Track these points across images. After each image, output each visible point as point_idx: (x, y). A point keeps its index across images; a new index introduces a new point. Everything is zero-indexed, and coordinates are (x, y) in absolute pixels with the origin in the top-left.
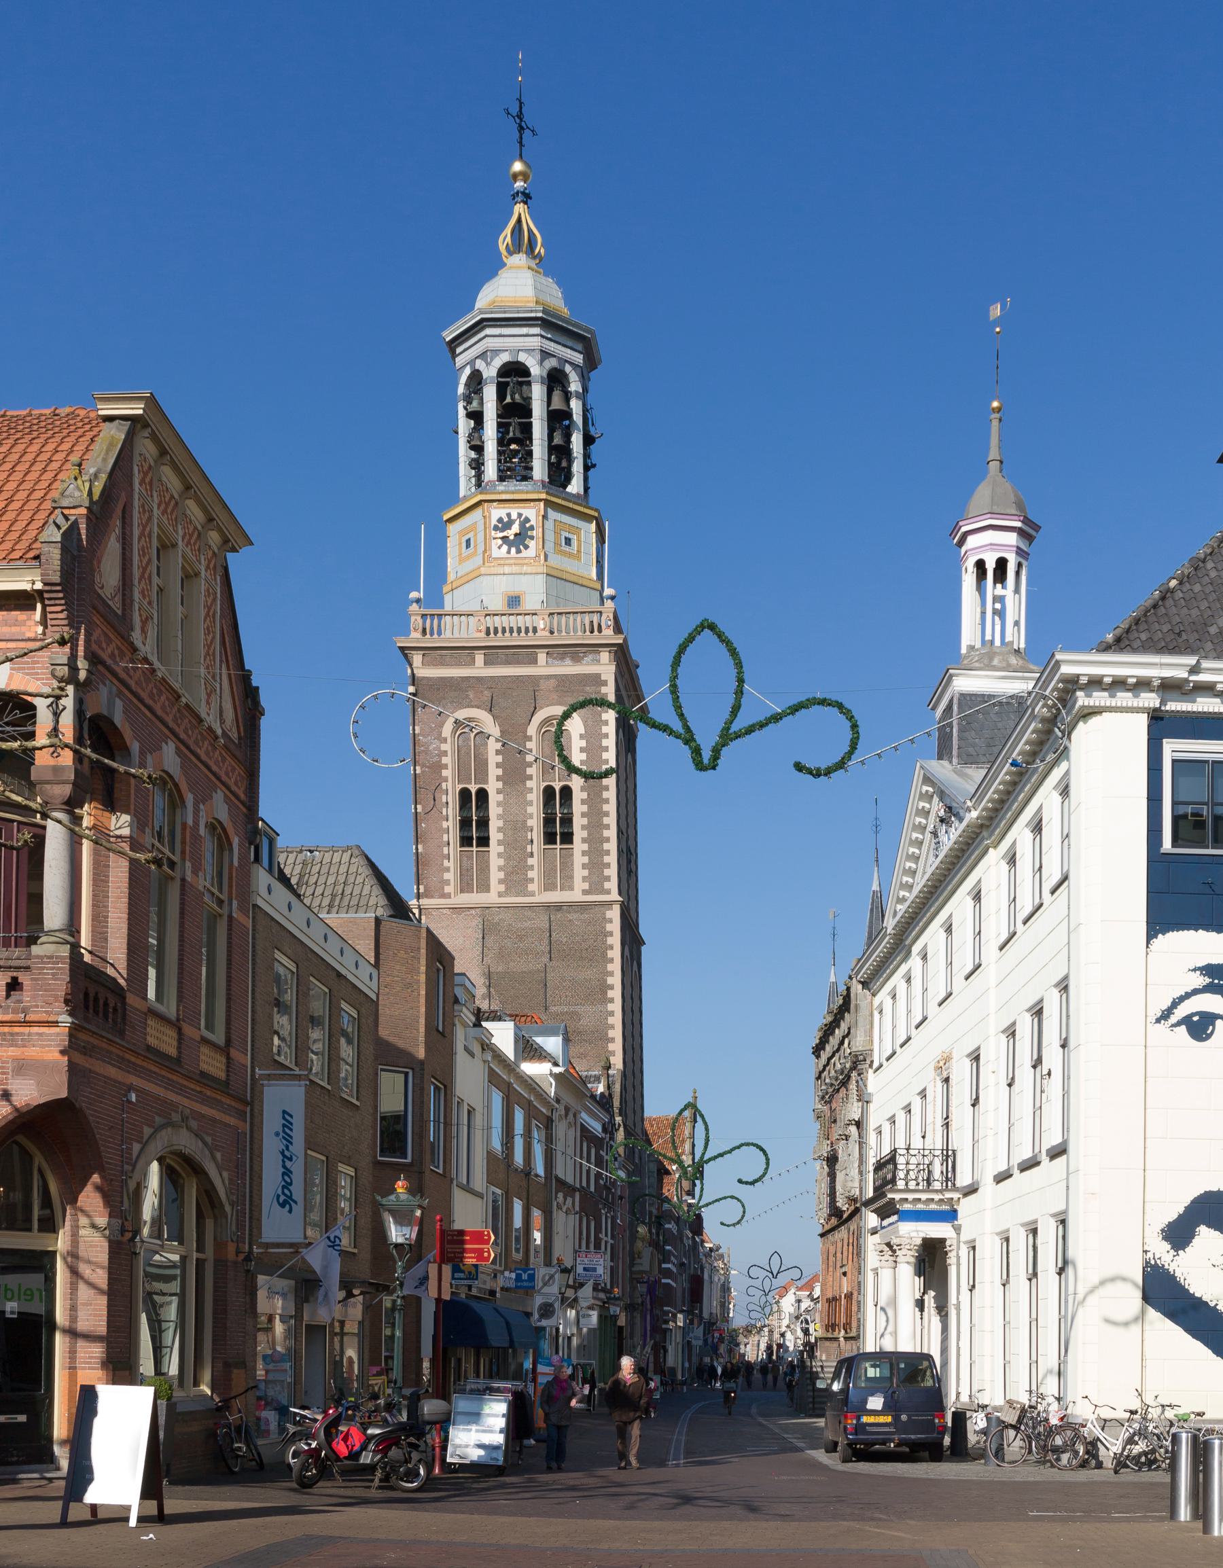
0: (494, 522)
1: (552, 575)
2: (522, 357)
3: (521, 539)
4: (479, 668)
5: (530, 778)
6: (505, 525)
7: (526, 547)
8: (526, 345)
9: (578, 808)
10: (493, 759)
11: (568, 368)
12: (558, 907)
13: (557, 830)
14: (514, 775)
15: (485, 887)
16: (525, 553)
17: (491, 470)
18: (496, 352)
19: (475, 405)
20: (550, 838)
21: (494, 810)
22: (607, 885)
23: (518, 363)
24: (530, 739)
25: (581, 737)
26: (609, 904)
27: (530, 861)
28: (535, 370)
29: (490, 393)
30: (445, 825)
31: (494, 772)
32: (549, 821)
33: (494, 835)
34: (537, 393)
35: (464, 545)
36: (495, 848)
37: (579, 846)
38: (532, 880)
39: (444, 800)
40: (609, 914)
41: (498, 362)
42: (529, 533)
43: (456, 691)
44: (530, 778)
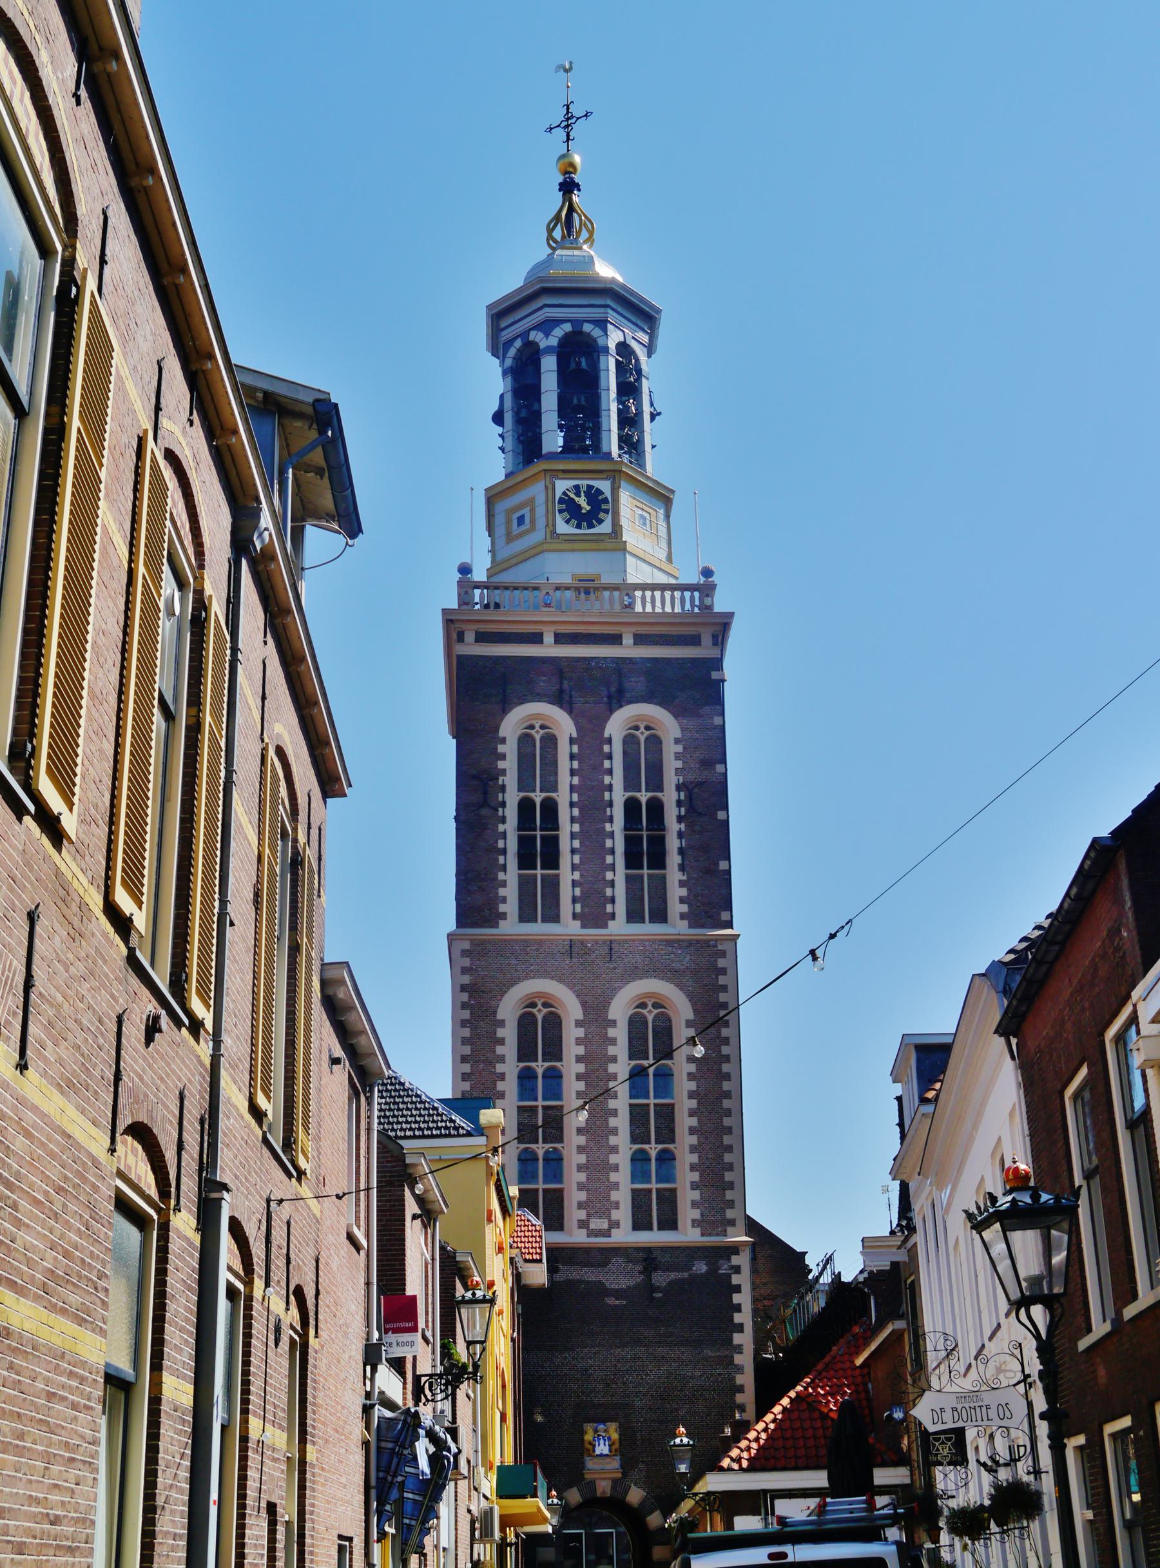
0: (558, 494)
2: (587, 328)
4: (549, 649)
7: (600, 521)
15: (553, 916)
18: (557, 322)
23: (581, 333)
29: (549, 364)
35: (515, 522)
41: (559, 332)
42: (603, 506)
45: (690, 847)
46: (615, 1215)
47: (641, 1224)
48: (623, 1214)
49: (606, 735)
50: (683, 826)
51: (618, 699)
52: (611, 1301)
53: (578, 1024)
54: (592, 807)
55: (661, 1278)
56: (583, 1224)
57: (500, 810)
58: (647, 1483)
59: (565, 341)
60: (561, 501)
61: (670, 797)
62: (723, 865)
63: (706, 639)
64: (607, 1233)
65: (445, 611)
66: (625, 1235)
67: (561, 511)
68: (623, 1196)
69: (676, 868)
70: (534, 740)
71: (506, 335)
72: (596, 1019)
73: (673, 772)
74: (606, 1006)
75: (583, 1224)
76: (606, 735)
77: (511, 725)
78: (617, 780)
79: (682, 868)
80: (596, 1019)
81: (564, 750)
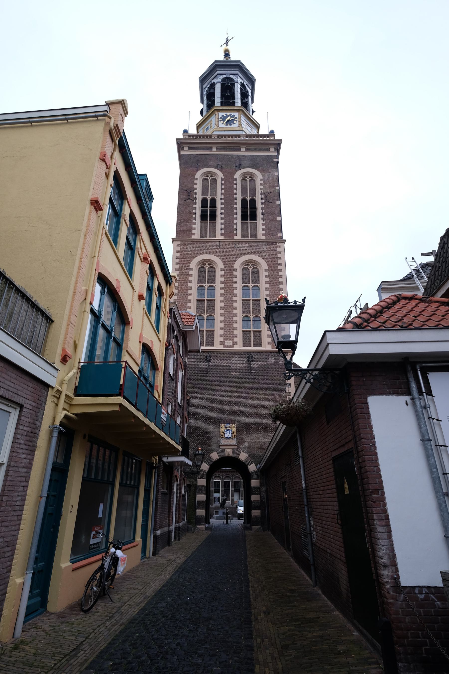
2: (231, 76)
4: (214, 152)
6: (223, 118)
31: (219, 191)
36: (219, 221)
45: (266, 212)
46: (235, 340)
47: (246, 343)
48: (239, 339)
49: (235, 178)
50: (263, 206)
51: (240, 167)
52: (233, 373)
53: (222, 270)
54: (229, 198)
55: (254, 365)
56: (222, 343)
57: (194, 200)
58: (249, 451)
59: (224, 80)
61: (258, 198)
62: (279, 218)
63: (272, 149)
64: (232, 346)
65: (177, 139)
66: (239, 347)
67: (220, 121)
68: (239, 333)
69: (261, 219)
70: (208, 180)
71: (204, 86)
72: (229, 269)
73: (260, 189)
74: (233, 263)
75: (222, 343)
76: (235, 178)
77: (199, 175)
78: (239, 191)
79: (263, 219)
80: (229, 269)
81: (219, 182)
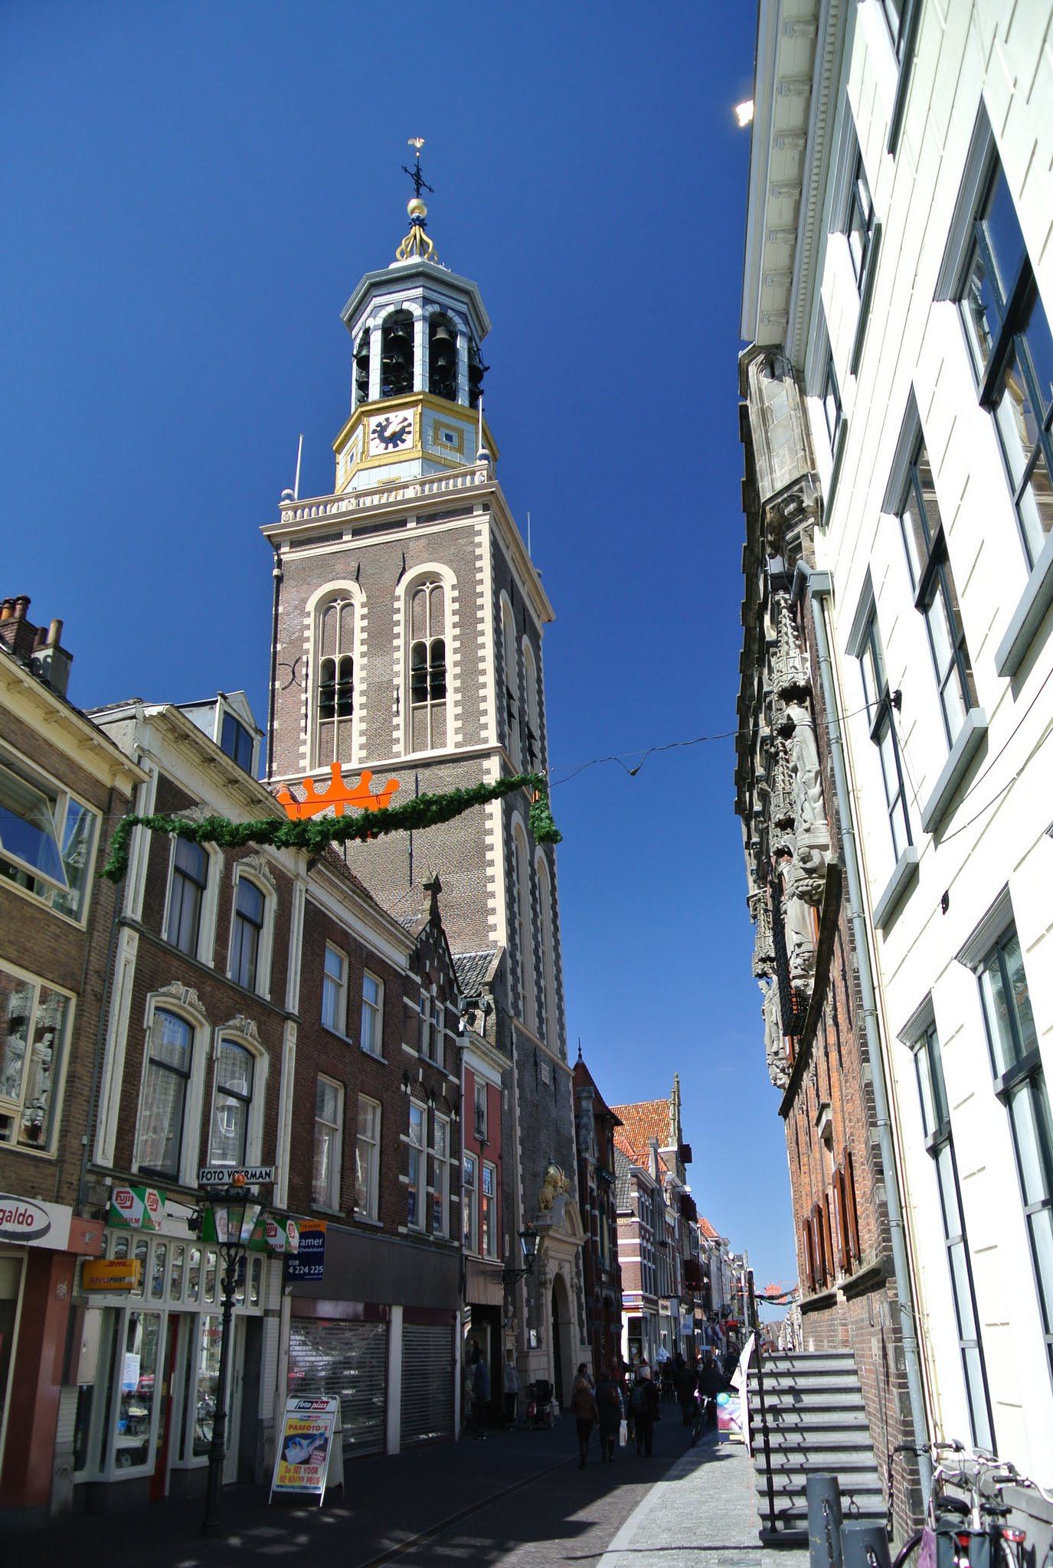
0: (373, 427)
1: (427, 460)
2: (406, 306)
3: (396, 438)
5: (398, 636)
6: (381, 430)
8: (411, 300)
9: (450, 658)
10: (359, 624)
11: (450, 313)
12: (426, 764)
13: (428, 683)
14: (380, 638)
16: (401, 446)
17: (375, 391)
19: (364, 353)
20: (419, 693)
21: (358, 674)
22: (483, 734)
24: (398, 599)
25: (454, 587)
26: (486, 754)
27: (396, 721)
28: (416, 310)
29: (376, 339)
30: (303, 697)
31: (359, 636)
32: (419, 677)
33: (357, 699)
34: (420, 330)
37: (451, 697)
38: (398, 740)
39: (304, 672)
40: (486, 764)
41: (384, 313)
43: (323, 568)
44: (398, 636)
60: (374, 432)
